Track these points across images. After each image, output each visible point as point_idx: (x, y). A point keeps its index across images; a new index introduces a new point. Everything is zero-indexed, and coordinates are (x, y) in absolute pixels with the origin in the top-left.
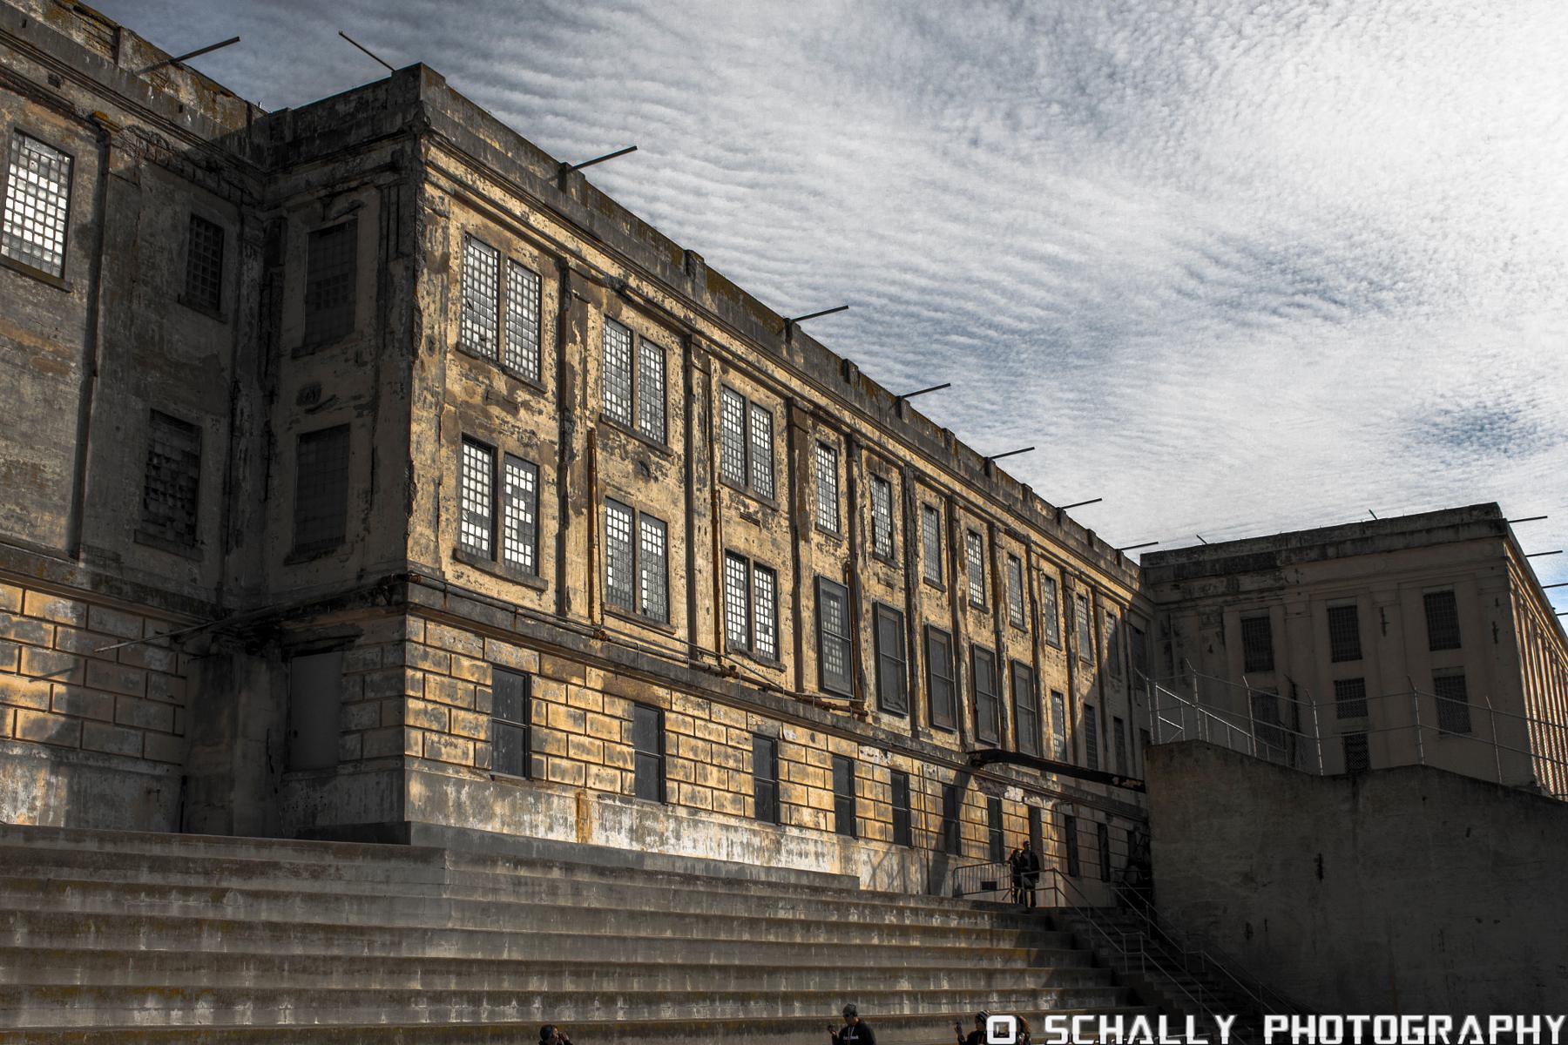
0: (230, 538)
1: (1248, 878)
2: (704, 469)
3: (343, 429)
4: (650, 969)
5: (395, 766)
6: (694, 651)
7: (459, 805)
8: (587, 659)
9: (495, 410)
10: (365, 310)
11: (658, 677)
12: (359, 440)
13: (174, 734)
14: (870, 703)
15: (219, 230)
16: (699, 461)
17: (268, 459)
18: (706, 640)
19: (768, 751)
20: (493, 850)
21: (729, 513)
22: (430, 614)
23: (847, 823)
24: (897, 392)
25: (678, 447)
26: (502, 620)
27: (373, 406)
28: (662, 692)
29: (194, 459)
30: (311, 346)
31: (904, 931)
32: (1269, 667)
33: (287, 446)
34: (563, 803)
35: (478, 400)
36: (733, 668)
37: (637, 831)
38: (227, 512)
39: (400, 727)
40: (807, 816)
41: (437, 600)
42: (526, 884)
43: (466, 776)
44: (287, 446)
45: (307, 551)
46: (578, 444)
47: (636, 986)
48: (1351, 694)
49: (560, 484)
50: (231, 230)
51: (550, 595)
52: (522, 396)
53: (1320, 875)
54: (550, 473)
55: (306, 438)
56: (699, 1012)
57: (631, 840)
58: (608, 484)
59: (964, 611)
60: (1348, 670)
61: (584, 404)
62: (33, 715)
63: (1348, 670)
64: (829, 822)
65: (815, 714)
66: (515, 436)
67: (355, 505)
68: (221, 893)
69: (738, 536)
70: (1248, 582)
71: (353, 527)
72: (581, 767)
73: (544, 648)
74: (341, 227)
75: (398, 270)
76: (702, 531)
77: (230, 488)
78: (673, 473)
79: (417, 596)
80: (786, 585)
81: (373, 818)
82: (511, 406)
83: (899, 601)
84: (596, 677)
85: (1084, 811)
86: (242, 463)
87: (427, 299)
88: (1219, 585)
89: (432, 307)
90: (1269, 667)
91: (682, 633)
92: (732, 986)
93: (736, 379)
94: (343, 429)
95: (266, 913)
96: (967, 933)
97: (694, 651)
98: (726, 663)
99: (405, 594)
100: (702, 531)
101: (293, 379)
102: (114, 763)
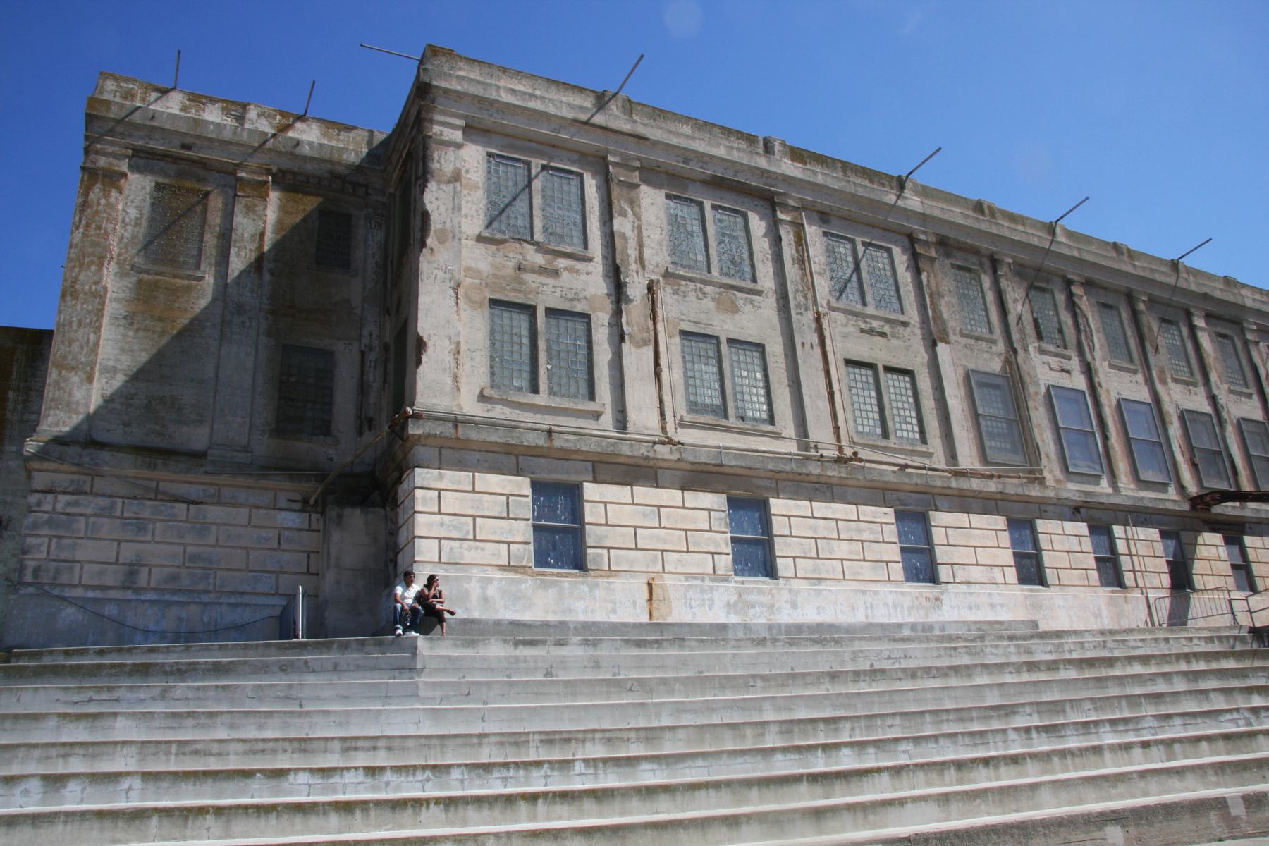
2: (805, 297)
7: (485, 600)
13: (308, 573)
16: (797, 291)
24: (1047, 220)
25: (767, 281)
36: (855, 454)
37: (736, 603)
42: (525, 661)
57: (728, 613)
58: (682, 320)
59: (1164, 382)
61: (641, 260)
62: (167, 570)
66: (558, 294)
72: (656, 557)
76: (807, 346)
80: (925, 383)
86: (372, 370)
87: (436, 203)
89: (442, 209)
100: (807, 346)
102: (246, 599)
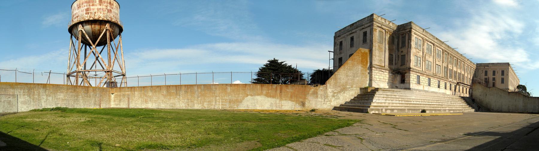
0: (396, 64)
3: (405, 55)
4: (429, 100)
8: (424, 74)
11: (430, 76)
12: (406, 56)
14: (448, 77)
15: (394, 37)
17: (398, 57)
18: (434, 72)
20: (417, 90)
22: (412, 71)
23: (446, 88)
26: (418, 71)
27: (408, 53)
29: (393, 58)
30: (401, 48)
31: (450, 98)
33: (400, 56)
34: (422, 86)
38: (395, 62)
39: (410, 80)
41: (413, 70)
44: (400, 56)
45: (401, 65)
47: (428, 101)
49: (423, 59)
50: (395, 37)
51: (422, 69)
55: (402, 55)
56: (433, 103)
65: (444, 79)
67: (406, 62)
68: (398, 93)
71: (406, 63)
73: (421, 73)
77: (395, 60)
79: (411, 70)
81: (408, 87)
84: (425, 76)
85: (468, 88)
92: (435, 102)
94: (405, 55)
95: (401, 95)
96: (455, 98)
101: (400, 50)
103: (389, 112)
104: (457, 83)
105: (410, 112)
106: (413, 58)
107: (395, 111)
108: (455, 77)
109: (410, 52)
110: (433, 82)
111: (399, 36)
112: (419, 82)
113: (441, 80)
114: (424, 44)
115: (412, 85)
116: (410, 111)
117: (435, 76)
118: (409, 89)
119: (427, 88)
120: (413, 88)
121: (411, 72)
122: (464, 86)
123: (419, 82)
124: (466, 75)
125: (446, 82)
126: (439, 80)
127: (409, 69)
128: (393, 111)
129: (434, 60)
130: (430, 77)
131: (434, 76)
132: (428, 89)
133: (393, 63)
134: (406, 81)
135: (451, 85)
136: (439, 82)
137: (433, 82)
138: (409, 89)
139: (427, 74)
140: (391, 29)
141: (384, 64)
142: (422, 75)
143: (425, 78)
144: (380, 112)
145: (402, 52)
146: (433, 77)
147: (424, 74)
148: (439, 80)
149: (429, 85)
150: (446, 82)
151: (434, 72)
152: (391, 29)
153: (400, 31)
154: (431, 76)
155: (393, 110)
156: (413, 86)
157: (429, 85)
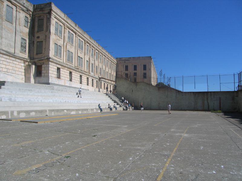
1: (126, 91)
3: (42, 41)
5: (48, 77)
6: (75, 66)
8: (65, 67)
9: (58, 41)
10: (45, 29)
12: (44, 42)
19: (81, 76)
21: (78, 52)
26: (58, 63)
27: (46, 40)
28: (72, 70)
32: (127, 70)
33: (35, 43)
35: (56, 39)
39: (49, 73)
40: (84, 83)
43: (54, 78)
45: (37, 54)
46: (65, 44)
48: (135, 74)
52: (60, 39)
53: (133, 91)
54: (62, 47)
55: (38, 42)
60: (135, 71)
63: (135, 71)
64: (86, 84)
67: (44, 50)
69: (79, 55)
70: (126, 62)
71: (43, 52)
74: (42, 19)
75: (48, 24)
78: (74, 47)
82: (59, 40)
83: (93, 62)
84: (66, 68)
88: (124, 62)
90: (127, 70)
91: (74, 64)
93: (80, 39)
94: (42, 41)
97: (75, 66)
98: (78, 68)
99: (49, 60)
103: (23, 115)
104: (99, 78)
105: (53, 115)
106: (52, 46)
107: (33, 114)
108: (99, 71)
109: (49, 38)
110: (75, 76)
111: (35, 18)
112: (59, 77)
113: (83, 75)
114: (65, 32)
115: (51, 78)
116: (53, 113)
117: (77, 70)
118: (48, 84)
119: (68, 83)
120: (52, 82)
121: (50, 63)
122: (106, 82)
123: (59, 77)
124: (107, 70)
125: (88, 77)
126: (81, 74)
127: (48, 59)
128: (30, 114)
129: (76, 51)
130: (72, 71)
131: (77, 70)
132: (69, 84)
133: (25, 51)
134: (43, 75)
135: (93, 80)
136: (81, 76)
137: (75, 76)
138: (48, 84)
139: (69, 67)
140: (24, 7)
141: (14, 49)
142: (62, 67)
143: (66, 71)
144: (10, 117)
145: (38, 37)
146: (74, 70)
147: (65, 67)
148: (81, 74)
149: (71, 80)
150: (88, 77)
151: (76, 65)
152: (24, 7)
153: (36, 12)
154: (73, 70)
155: (28, 112)
156: (52, 81)
157: (71, 80)
